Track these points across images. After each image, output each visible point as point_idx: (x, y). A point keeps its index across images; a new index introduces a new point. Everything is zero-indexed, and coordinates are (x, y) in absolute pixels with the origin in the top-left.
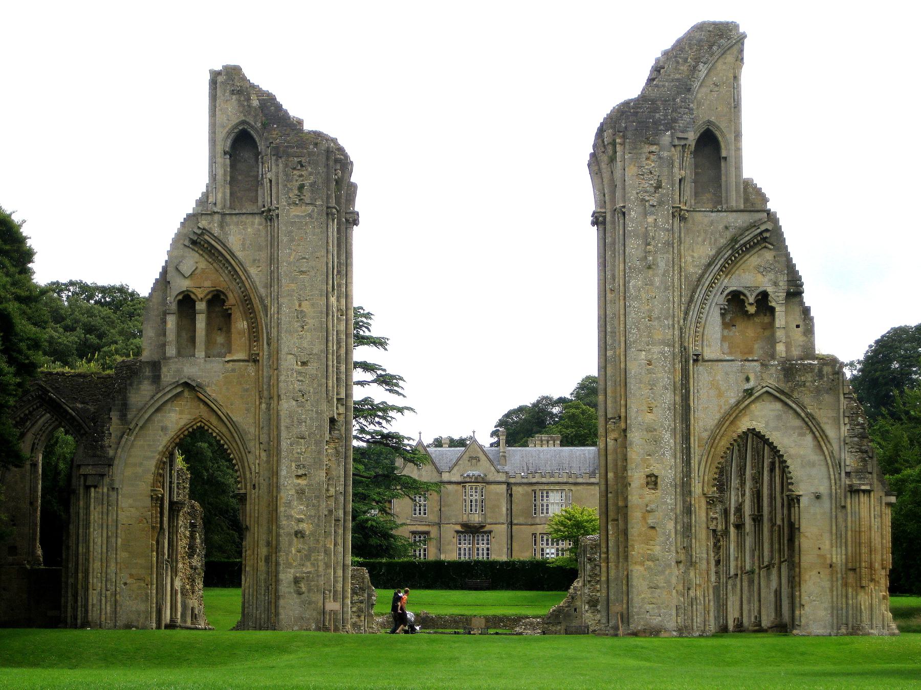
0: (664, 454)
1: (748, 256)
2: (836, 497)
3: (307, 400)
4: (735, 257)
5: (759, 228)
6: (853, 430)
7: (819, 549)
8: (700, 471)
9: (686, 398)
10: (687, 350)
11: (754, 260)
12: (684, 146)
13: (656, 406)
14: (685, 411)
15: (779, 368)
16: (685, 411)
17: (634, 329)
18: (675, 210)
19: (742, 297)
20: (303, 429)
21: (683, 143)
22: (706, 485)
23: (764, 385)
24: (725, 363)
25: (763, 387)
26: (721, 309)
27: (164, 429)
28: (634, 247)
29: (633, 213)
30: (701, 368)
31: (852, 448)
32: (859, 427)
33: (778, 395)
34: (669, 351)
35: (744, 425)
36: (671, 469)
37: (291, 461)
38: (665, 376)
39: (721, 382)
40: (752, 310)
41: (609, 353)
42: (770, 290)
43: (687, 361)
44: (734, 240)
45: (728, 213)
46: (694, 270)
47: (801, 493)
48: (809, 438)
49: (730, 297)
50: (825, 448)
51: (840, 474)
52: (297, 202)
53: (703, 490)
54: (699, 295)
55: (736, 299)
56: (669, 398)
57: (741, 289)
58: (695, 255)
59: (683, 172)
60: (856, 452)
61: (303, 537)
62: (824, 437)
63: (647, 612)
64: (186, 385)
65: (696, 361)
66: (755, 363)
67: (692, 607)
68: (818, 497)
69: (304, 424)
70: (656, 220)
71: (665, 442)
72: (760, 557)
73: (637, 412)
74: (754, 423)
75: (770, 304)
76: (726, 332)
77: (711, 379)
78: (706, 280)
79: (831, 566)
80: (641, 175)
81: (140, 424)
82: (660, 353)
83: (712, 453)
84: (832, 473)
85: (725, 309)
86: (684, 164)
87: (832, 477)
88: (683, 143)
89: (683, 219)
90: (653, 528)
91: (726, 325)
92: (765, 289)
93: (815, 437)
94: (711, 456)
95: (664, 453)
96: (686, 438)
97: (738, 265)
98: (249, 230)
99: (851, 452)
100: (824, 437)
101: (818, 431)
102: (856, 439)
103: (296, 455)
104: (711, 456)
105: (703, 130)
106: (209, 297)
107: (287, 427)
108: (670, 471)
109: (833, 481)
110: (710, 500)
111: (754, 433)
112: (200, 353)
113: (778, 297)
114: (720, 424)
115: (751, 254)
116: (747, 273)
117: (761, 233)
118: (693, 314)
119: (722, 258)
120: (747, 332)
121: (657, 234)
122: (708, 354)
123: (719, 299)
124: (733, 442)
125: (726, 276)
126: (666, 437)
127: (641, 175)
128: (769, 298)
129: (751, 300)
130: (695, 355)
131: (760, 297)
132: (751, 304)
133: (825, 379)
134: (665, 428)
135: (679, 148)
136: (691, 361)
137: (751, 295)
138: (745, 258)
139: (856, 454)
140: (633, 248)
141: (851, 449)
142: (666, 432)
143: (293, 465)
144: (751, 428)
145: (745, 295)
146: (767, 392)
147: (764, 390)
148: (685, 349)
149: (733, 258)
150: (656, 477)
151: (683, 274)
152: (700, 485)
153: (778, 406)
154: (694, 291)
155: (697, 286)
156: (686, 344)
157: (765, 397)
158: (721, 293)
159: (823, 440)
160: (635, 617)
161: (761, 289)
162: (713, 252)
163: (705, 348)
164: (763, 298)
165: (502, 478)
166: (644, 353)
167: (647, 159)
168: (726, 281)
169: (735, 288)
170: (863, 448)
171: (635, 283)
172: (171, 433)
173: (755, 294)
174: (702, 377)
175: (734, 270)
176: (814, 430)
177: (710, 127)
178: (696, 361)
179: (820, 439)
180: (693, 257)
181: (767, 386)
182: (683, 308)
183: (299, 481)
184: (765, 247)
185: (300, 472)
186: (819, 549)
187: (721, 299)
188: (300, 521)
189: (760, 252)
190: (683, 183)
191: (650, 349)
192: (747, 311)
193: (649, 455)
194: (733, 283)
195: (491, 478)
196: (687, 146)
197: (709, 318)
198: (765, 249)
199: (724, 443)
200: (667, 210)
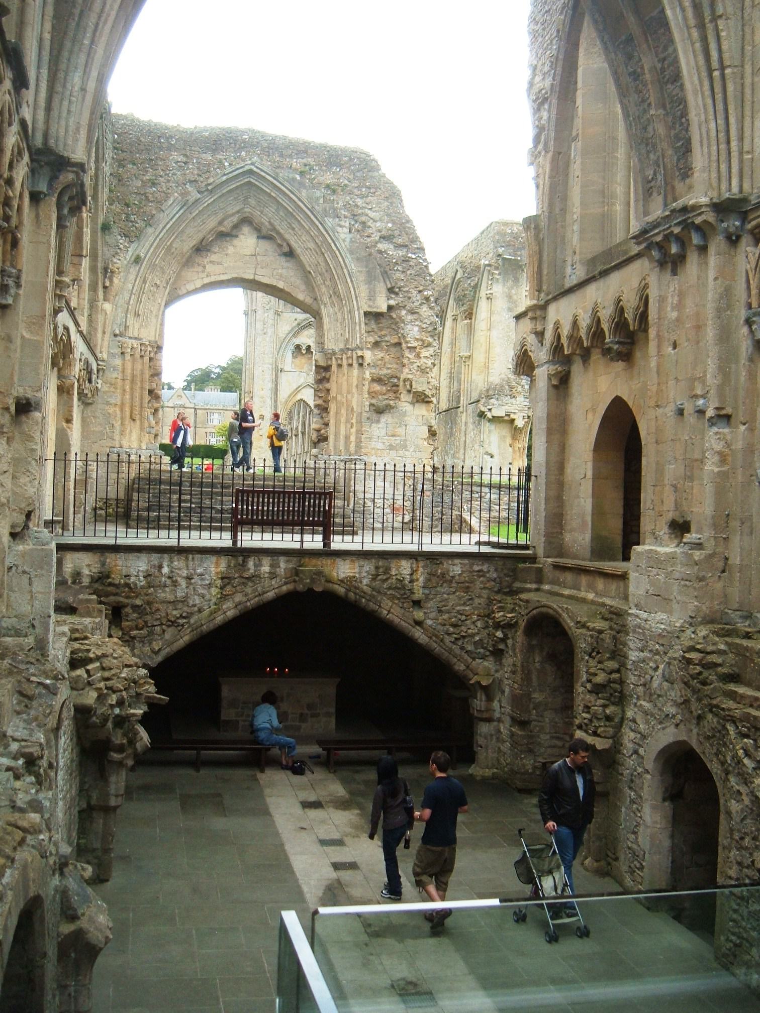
9: (276, 385)
14: (276, 391)
16: (276, 391)
28: (259, 325)
30: (283, 374)
35: (299, 397)
38: (269, 376)
40: (304, 352)
44: (299, 324)
46: (282, 335)
54: (283, 346)
55: (298, 347)
56: (269, 385)
72: (304, 448)
89: (279, 315)
91: (294, 357)
96: (276, 401)
111: (302, 400)
114: (289, 397)
118: (281, 353)
120: (301, 360)
164: (309, 347)
165: (192, 406)
171: (259, 339)
174: (283, 378)
187: (292, 348)
194: (297, 341)
195: (187, 405)
199: (291, 404)
200: (272, 312)
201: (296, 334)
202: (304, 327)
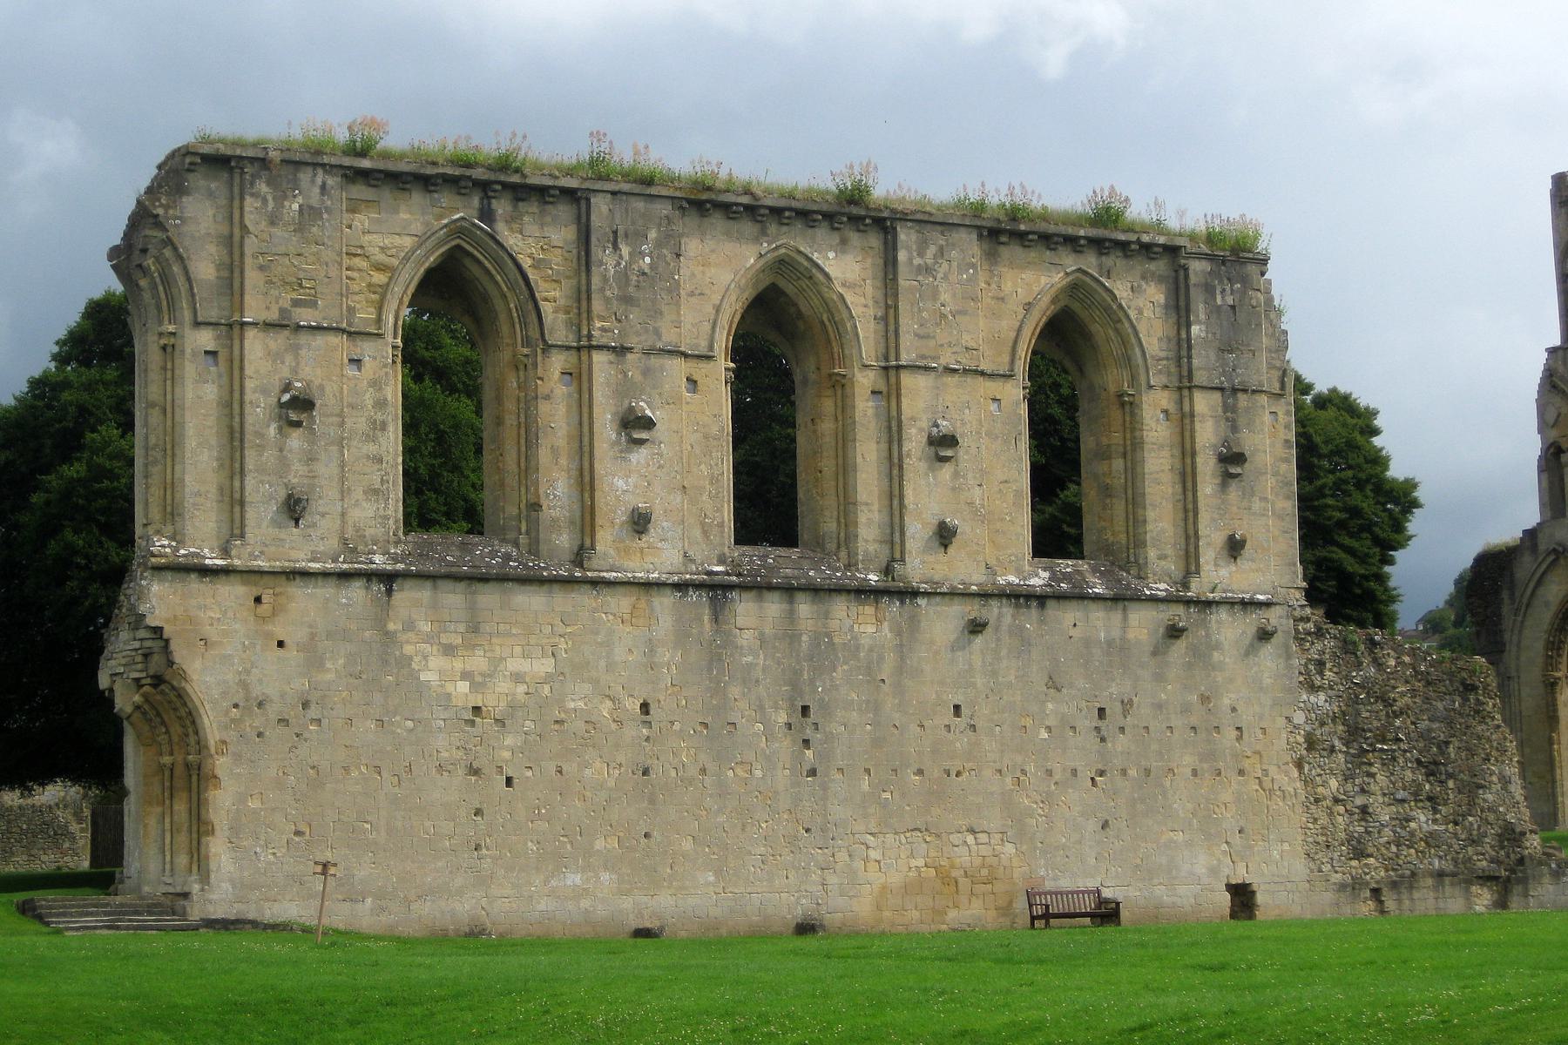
27: (1547, 604)
64: (1554, 550)
81: (1525, 601)
172: (1553, 608)
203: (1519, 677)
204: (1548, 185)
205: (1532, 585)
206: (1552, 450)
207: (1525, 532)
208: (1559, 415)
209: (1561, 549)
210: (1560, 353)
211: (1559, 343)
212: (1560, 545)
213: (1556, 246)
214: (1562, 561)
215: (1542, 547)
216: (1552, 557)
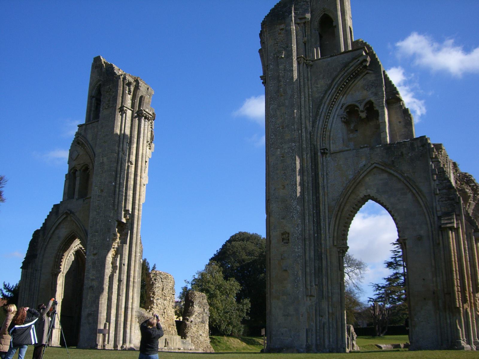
0: (293, 217)
1: (356, 81)
2: (433, 238)
3: (101, 211)
4: (347, 83)
5: (359, 60)
6: (442, 184)
7: (424, 279)
8: (330, 230)
10: (316, 147)
11: (360, 83)
12: (305, 23)
13: (287, 184)
15: (382, 149)
17: (272, 136)
18: (299, 59)
19: (356, 108)
20: (98, 227)
21: (303, 21)
22: (335, 239)
23: (372, 162)
24: (345, 152)
25: (372, 164)
26: (341, 118)
29: (271, 66)
31: (442, 198)
32: (446, 181)
33: (383, 168)
34: (295, 145)
36: (298, 227)
37: (91, 246)
39: (342, 166)
40: (363, 115)
41: (267, 158)
42: (373, 99)
43: (316, 154)
45: (338, 56)
47: (406, 238)
48: (409, 196)
49: (348, 110)
50: (421, 201)
51: (434, 218)
52: (107, 108)
53: (333, 243)
57: (353, 103)
58: (319, 86)
59: (306, 39)
60: (446, 200)
61: (93, 290)
62: (420, 193)
63: (282, 334)
64: (66, 213)
65: (323, 154)
66: (366, 149)
67: (324, 330)
68: (420, 238)
69: (98, 224)
70: (285, 66)
71: (294, 208)
73: (275, 190)
74: (368, 191)
75: (375, 109)
76: (351, 136)
77: (336, 165)
78: (327, 100)
79: (434, 293)
80: (276, 43)
81: (49, 235)
82: (288, 148)
83: (339, 216)
84: (428, 219)
85: (344, 118)
86: (307, 33)
87: (429, 222)
88: (303, 21)
90: (286, 270)
92: (369, 99)
93: (413, 195)
94: (338, 218)
95: (293, 216)
96: (317, 206)
97: (351, 88)
98: (96, 130)
99: (442, 201)
100: (420, 193)
101: (414, 189)
102: (445, 191)
103: (93, 243)
104: (338, 218)
105: (322, 15)
106: (84, 168)
107: (91, 227)
108: (297, 228)
109: (429, 225)
110: (340, 250)
112: (76, 196)
113: (379, 102)
115: (358, 79)
116: (357, 92)
117: (361, 63)
118: (320, 124)
119: (336, 84)
121: (286, 74)
122: (333, 148)
123: (338, 112)
124: (355, 206)
125: (343, 96)
126: (294, 204)
127: (276, 43)
128: (374, 105)
129: (361, 108)
130: (322, 149)
131: (368, 106)
132: (362, 112)
133: (417, 150)
134: (293, 198)
135: (302, 25)
136: (319, 154)
137: (361, 105)
138: (355, 83)
139: (446, 202)
140: (271, 86)
141: (442, 199)
142: (294, 201)
143: (92, 248)
144: (367, 194)
145: (358, 107)
146: (375, 167)
147: (373, 166)
148: (314, 146)
149: (345, 84)
150: (289, 233)
151: (311, 98)
152: (331, 239)
153: (385, 176)
154: (319, 108)
155: (320, 105)
156: (315, 143)
157: (375, 170)
158: (341, 108)
159: (419, 195)
160: (274, 338)
161: (367, 100)
162: (330, 82)
163: (331, 145)
166: (279, 150)
167: (280, 34)
168: (343, 100)
169: (350, 104)
170: (451, 196)
173: (363, 104)
175: (348, 92)
176: (412, 189)
177: (326, 13)
178: (323, 154)
179: (417, 195)
180: (317, 87)
181: (375, 163)
182: (311, 120)
183: (95, 258)
184: (367, 73)
185: (95, 252)
186: (424, 279)
188: (92, 280)
189: (364, 77)
190: (307, 45)
191: (283, 147)
192: (360, 117)
193: (283, 219)
194: (346, 100)
196: (307, 22)
197: (334, 125)
198: (368, 75)
201: (344, 88)
202: (355, 75)
203: (41, 270)
204: (92, 61)
205: (53, 229)
206: (72, 171)
207: (55, 206)
208: (79, 155)
209: (69, 212)
210: (84, 127)
211: (84, 123)
212: (69, 210)
213: (91, 84)
214: (69, 218)
215: (61, 211)
216: (64, 216)
